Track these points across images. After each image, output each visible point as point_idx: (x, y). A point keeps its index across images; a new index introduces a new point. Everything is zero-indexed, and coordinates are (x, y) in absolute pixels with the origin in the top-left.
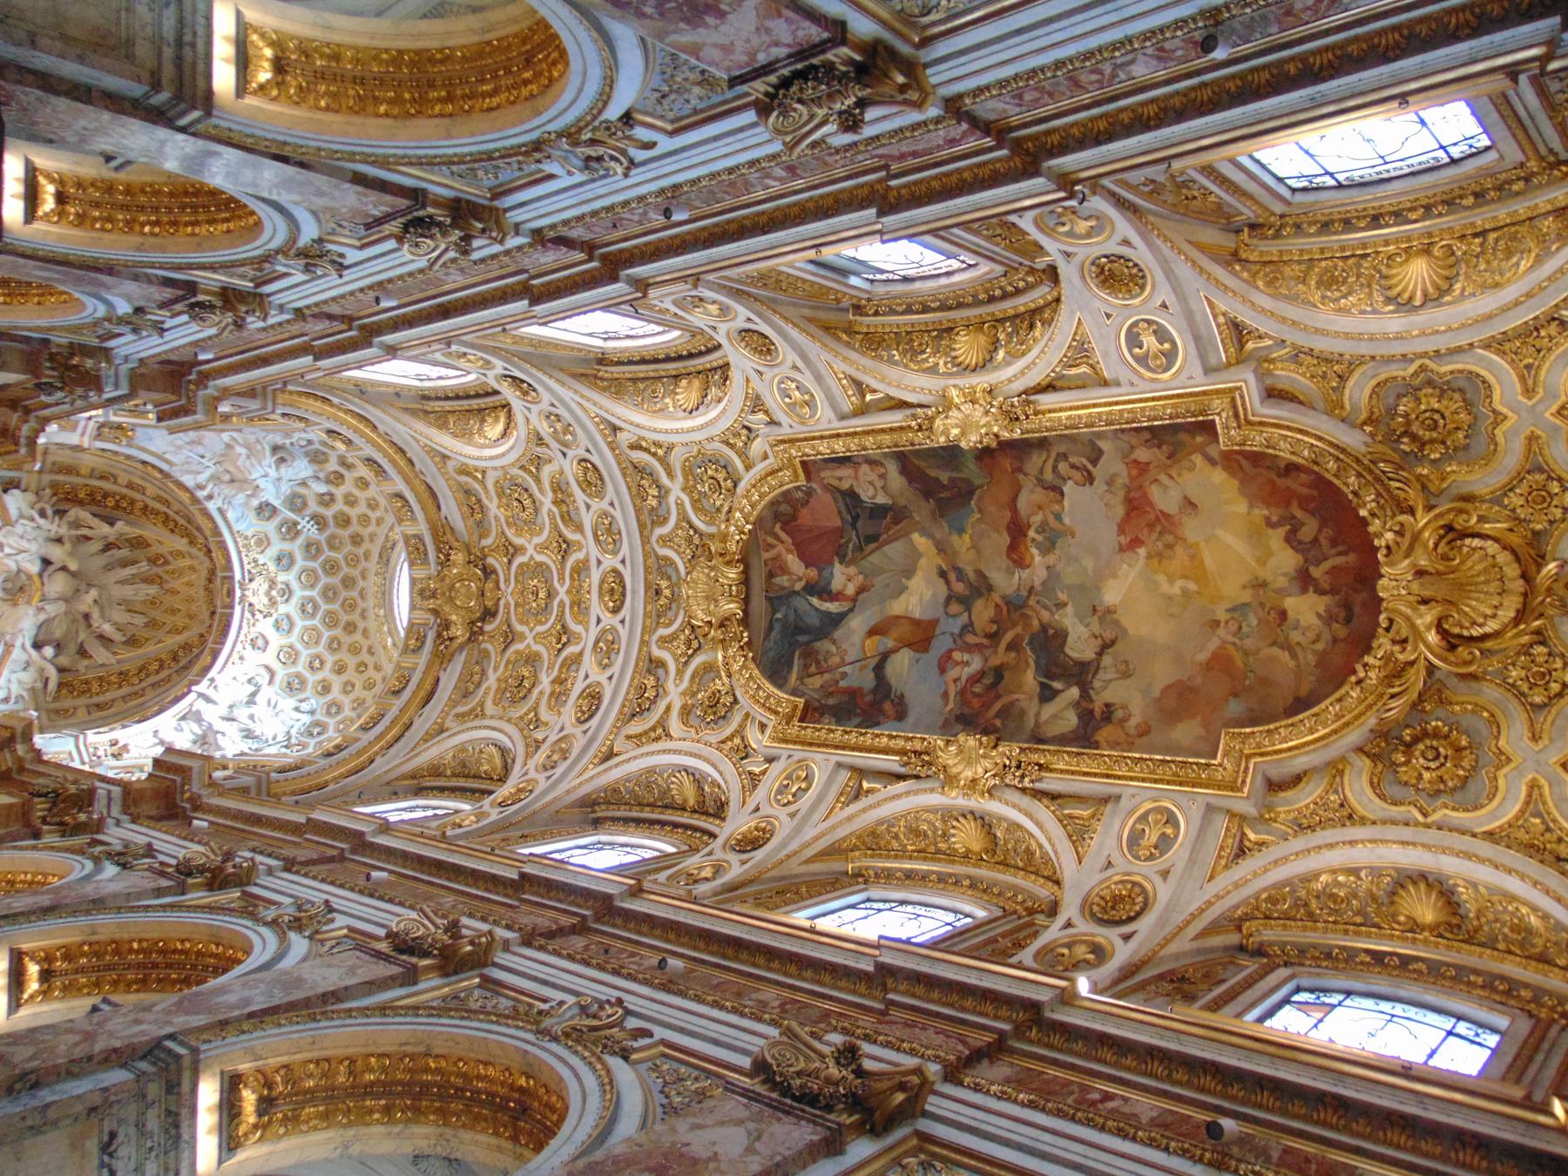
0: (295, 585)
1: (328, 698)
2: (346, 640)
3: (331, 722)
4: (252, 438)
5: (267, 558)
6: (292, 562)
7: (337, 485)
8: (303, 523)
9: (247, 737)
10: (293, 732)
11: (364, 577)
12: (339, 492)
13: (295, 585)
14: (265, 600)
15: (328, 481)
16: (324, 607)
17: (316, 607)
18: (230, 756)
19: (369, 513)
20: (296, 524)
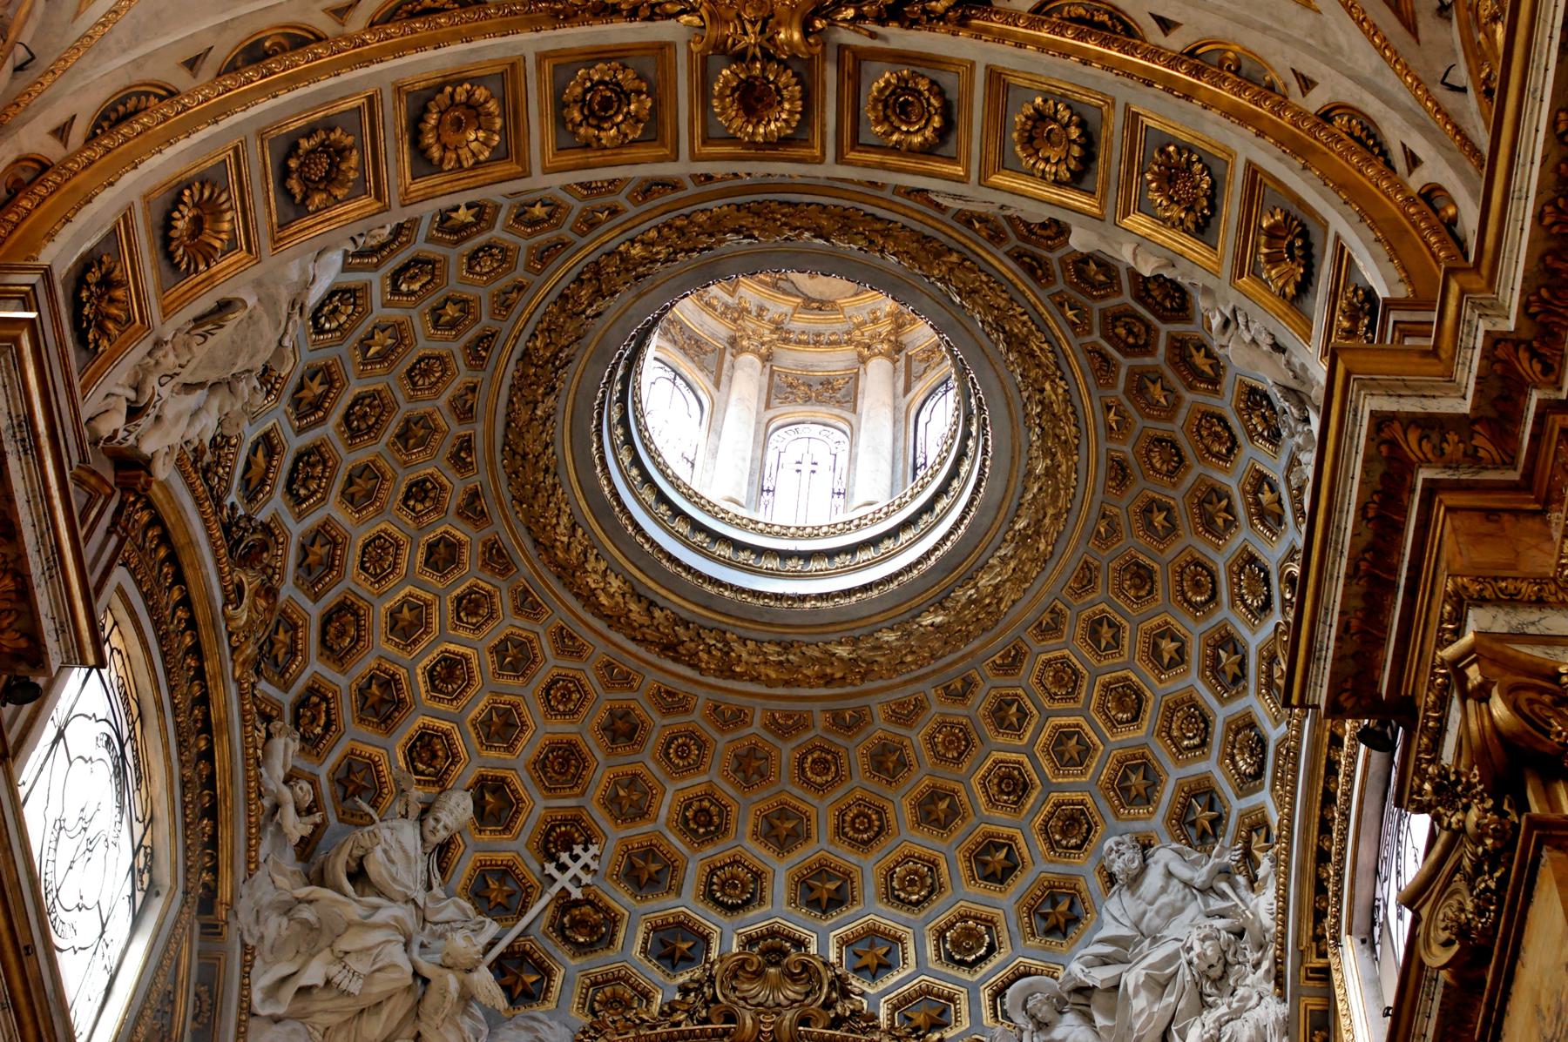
0: (755, 921)
1: (1099, 805)
2: (920, 779)
3: (1174, 775)
4: (275, 926)
5: (664, 987)
6: (683, 927)
7: (454, 757)
8: (563, 880)
9: (1219, 981)
10: (1200, 876)
11: (738, 718)
12: (474, 760)
13: (755, 921)
14: (790, 992)
15: (440, 780)
16: (821, 846)
17: (822, 870)
18: (1284, 1009)
19: (542, 676)
20: (565, 903)
